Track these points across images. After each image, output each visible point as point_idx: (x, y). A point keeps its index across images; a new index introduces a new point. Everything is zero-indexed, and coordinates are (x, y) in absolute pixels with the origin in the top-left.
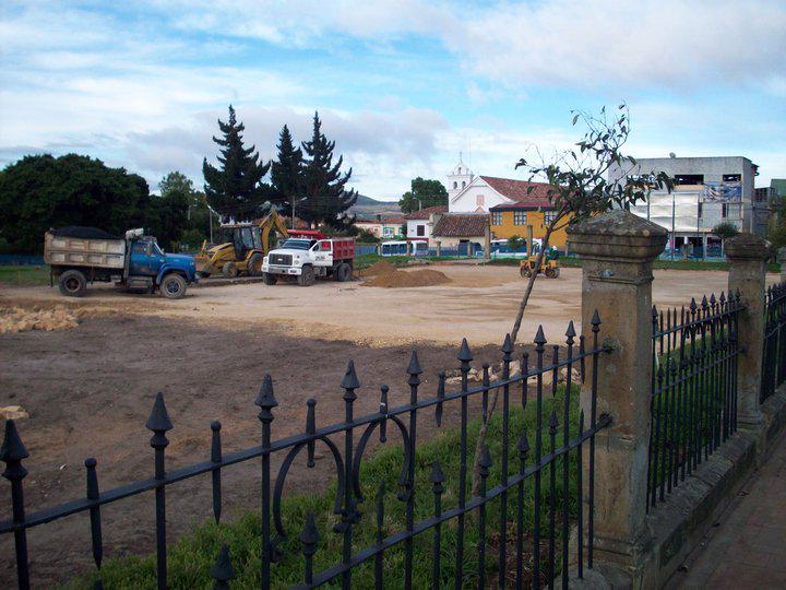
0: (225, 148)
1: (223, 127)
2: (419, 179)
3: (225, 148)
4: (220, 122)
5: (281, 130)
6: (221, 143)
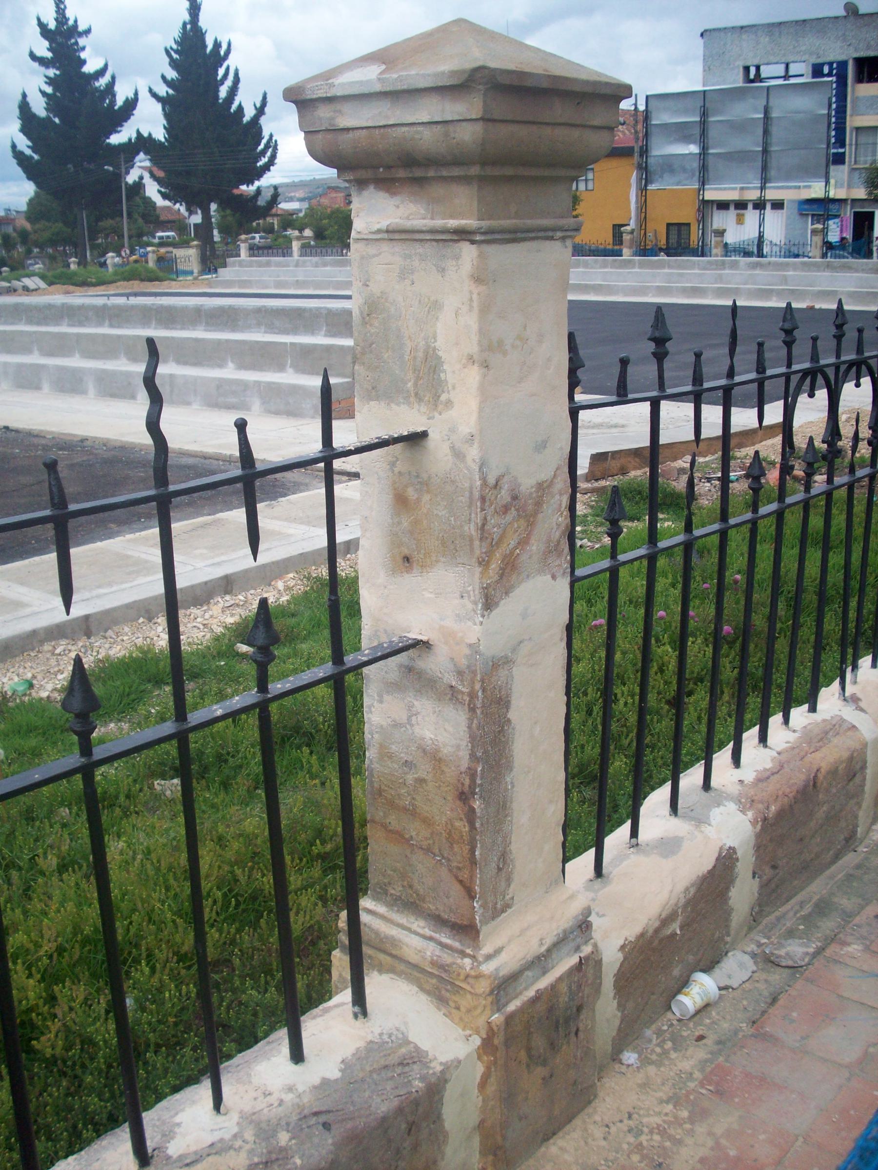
0: (52, 72)
3: (52, 72)
4: (42, 25)
6: (42, 61)
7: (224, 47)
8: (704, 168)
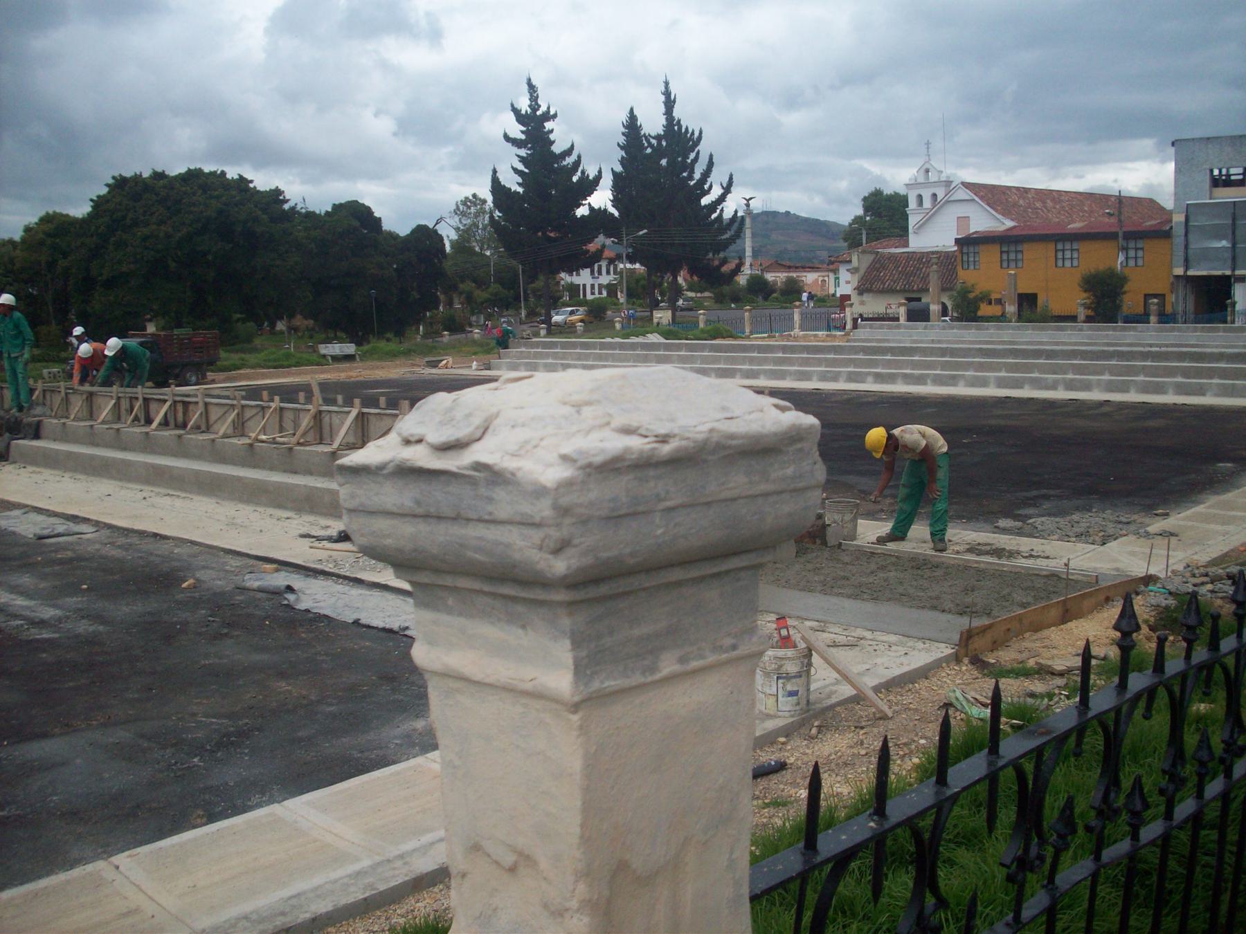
0: (523, 152)
1: (520, 118)
2: (877, 194)
3: (523, 152)
5: (623, 117)
7: (696, 134)
8: (1234, 259)
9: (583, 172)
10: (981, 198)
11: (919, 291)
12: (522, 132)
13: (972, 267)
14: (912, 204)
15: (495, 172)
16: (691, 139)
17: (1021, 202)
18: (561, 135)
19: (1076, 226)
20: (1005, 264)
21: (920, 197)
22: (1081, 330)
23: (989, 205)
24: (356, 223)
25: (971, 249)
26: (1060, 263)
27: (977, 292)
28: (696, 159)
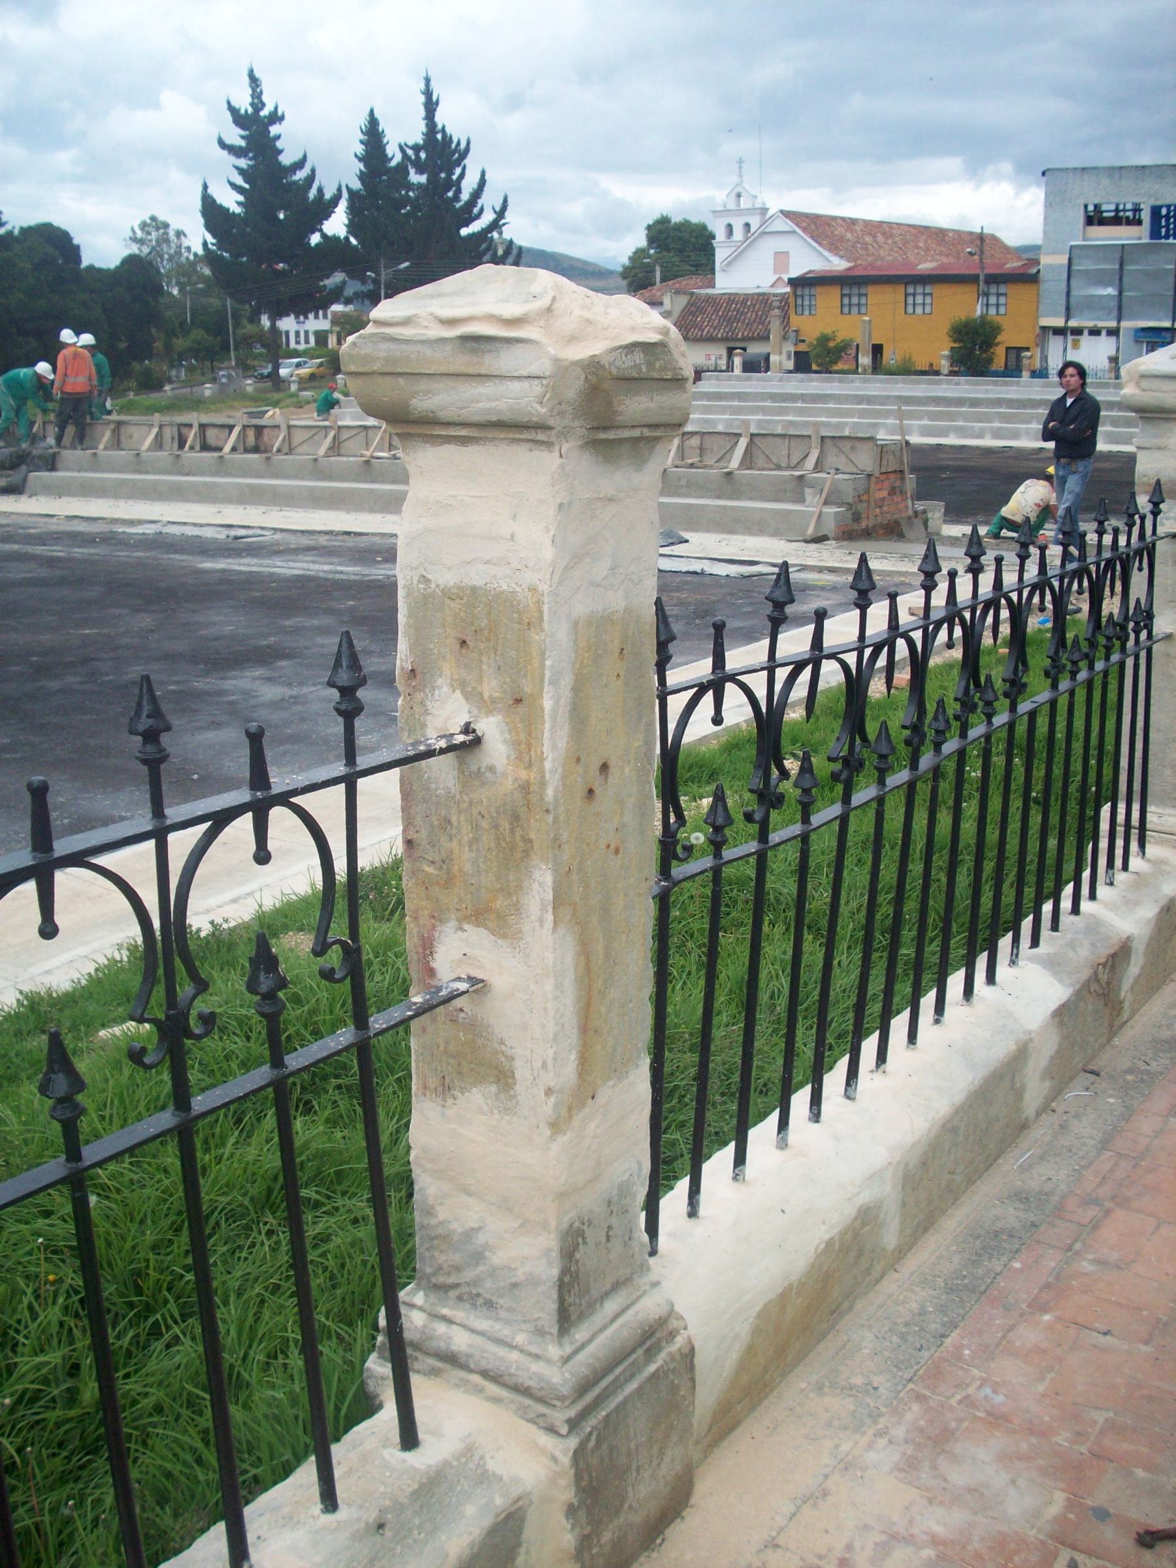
0: (243, 163)
1: (239, 119)
2: (664, 221)
3: (243, 163)
4: (233, 110)
5: (362, 120)
7: (463, 146)
8: (1120, 308)
9: (320, 190)
10: (804, 229)
11: (744, 339)
12: (242, 137)
13: (807, 312)
14: (720, 235)
15: (205, 187)
16: (457, 149)
17: (849, 235)
18: (290, 143)
19: (926, 267)
20: (846, 310)
21: (730, 228)
22: (957, 384)
23: (813, 238)
24: (50, 250)
25: (807, 291)
26: (910, 310)
27: (838, 340)
28: (462, 176)
